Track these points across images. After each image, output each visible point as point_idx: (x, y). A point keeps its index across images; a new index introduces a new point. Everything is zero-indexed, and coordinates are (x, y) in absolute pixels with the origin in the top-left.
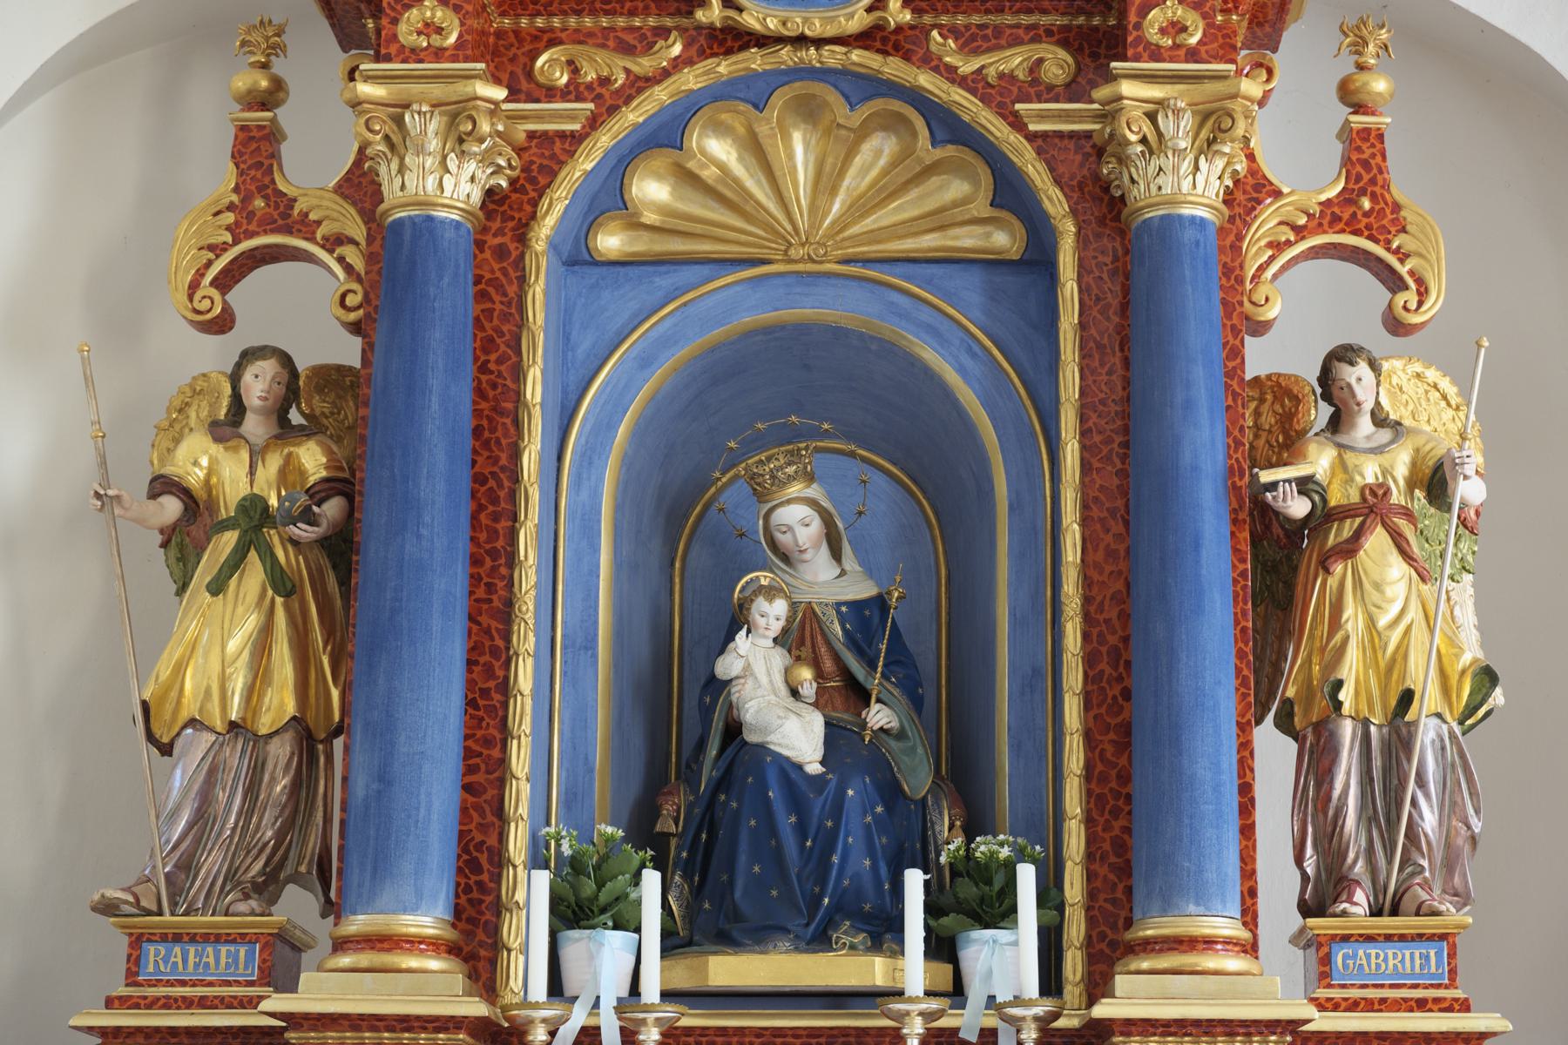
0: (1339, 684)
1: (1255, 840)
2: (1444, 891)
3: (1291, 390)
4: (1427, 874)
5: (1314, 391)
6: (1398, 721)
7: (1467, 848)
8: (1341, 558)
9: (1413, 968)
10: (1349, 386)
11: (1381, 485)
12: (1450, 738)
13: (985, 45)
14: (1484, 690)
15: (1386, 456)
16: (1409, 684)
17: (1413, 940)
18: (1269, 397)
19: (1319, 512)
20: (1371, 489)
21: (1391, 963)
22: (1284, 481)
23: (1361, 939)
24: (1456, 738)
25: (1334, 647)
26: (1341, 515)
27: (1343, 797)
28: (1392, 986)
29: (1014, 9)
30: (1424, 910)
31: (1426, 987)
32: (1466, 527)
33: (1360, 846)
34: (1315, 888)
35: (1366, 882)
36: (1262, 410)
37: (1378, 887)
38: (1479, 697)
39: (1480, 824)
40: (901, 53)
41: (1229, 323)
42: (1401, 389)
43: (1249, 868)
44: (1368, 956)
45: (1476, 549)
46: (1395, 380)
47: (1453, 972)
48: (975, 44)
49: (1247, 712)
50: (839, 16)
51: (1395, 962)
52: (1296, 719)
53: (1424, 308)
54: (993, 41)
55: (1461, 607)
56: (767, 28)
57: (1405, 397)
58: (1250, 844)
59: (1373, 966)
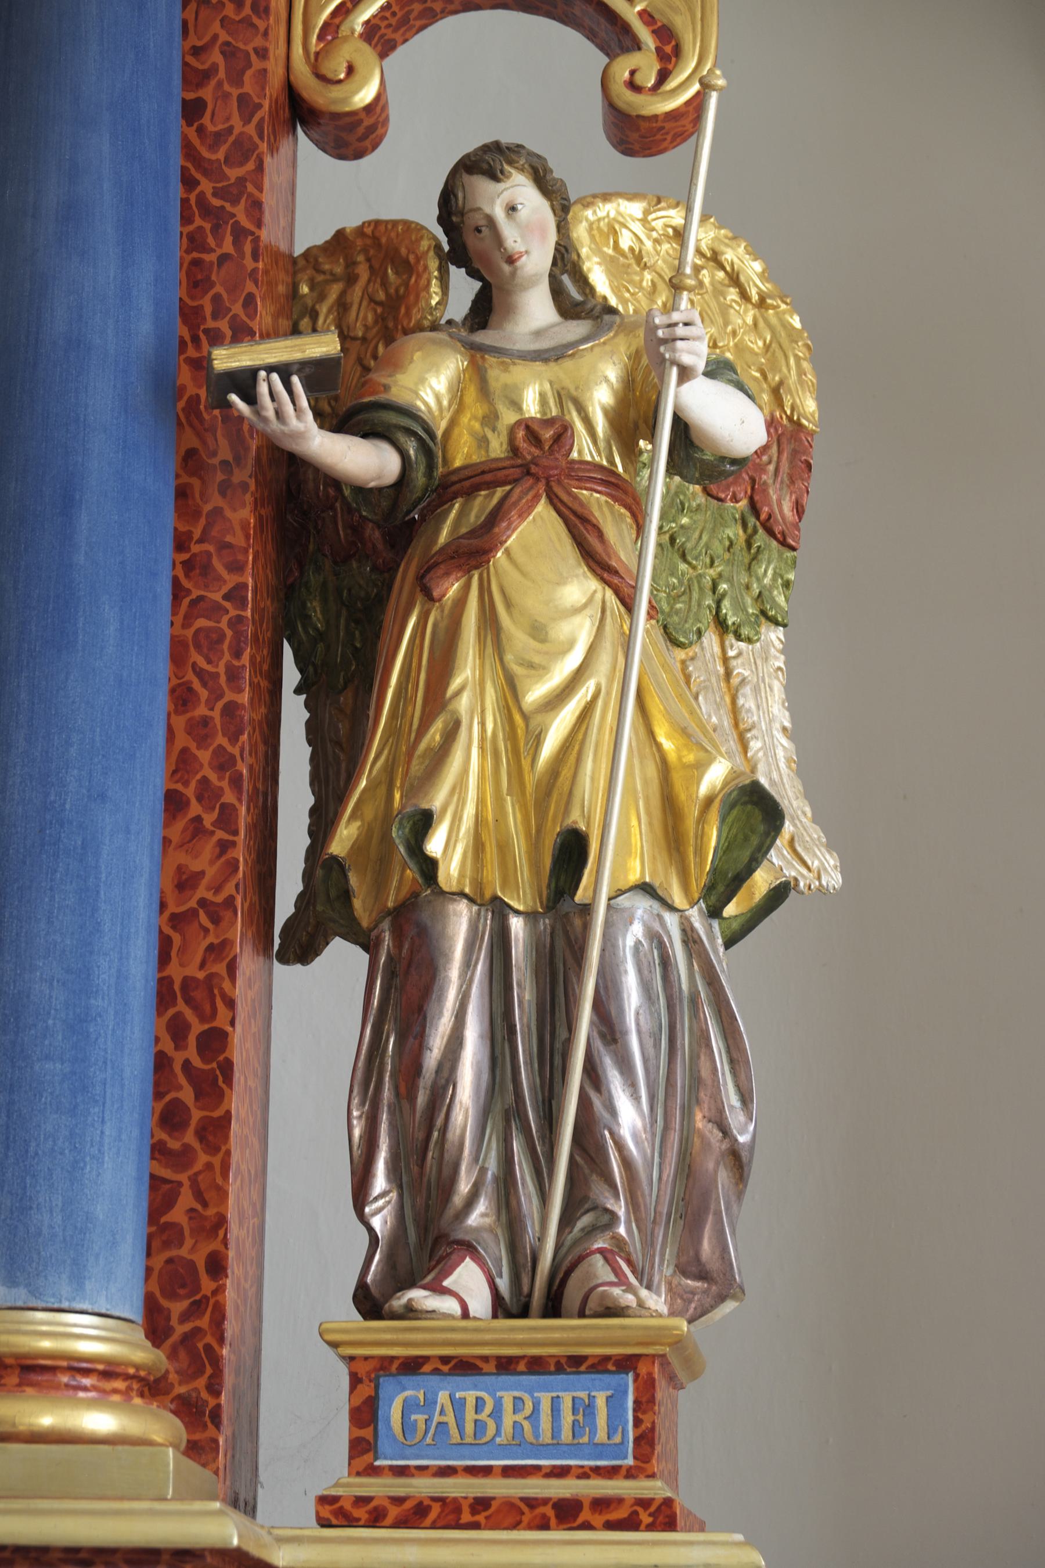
0: (424, 822)
1: (228, 1153)
2: (682, 1270)
3: (397, 250)
4: (622, 1230)
5: (438, 247)
6: (565, 906)
7: (723, 1178)
8: (459, 567)
9: (556, 1432)
10: (491, 222)
11: (549, 422)
12: (685, 942)
14: (755, 841)
15: (568, 364)
16: (576, 818)
17: (559, 1369)
18: (363, 272)
19: (419, 478)
20: (528, 428)
21: (508, 1419)
22: (270, 369)
23: (445, 1368)
24: (698, 941)
25: (428, 749)
26: (467, 484)
27: (447, 1065)
28: (508, 1472)
30: (592, 1305)
31: (584, 1474)
32: (770, 532)
33: (483, 1171)
34: (390, 1259)
35: (497, 1250)
36: (349, 300)
37: (521, 1260)
38: (746, 855)
39: (751, 1128)
41: (235, 92)
42: (639, 258)
43: (211, 1212)
44: (459, 1406)
45: (791, 576)
46: (626, 241)
47: (645, 1441)
49: (226, 880)
51: (519, 1418)
52: (357, 903)
53: (672, 84)
55: (756, 690)
57: (648, 276)
58: (216, 1161)
59: (469, 1428)
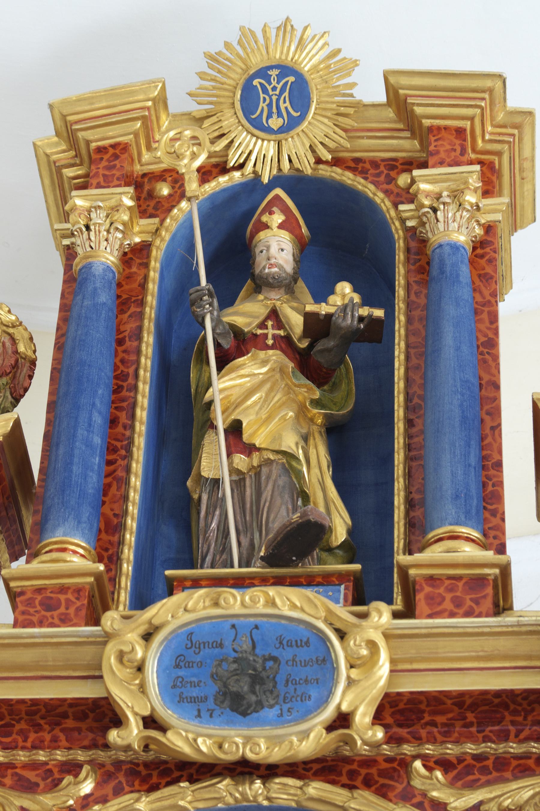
13: (484, 778)
29: (522, 736)
40: (373, 788)
48: (471, 777)
50: (291, 735)
54: (495, 774)
56: (199, 750)
